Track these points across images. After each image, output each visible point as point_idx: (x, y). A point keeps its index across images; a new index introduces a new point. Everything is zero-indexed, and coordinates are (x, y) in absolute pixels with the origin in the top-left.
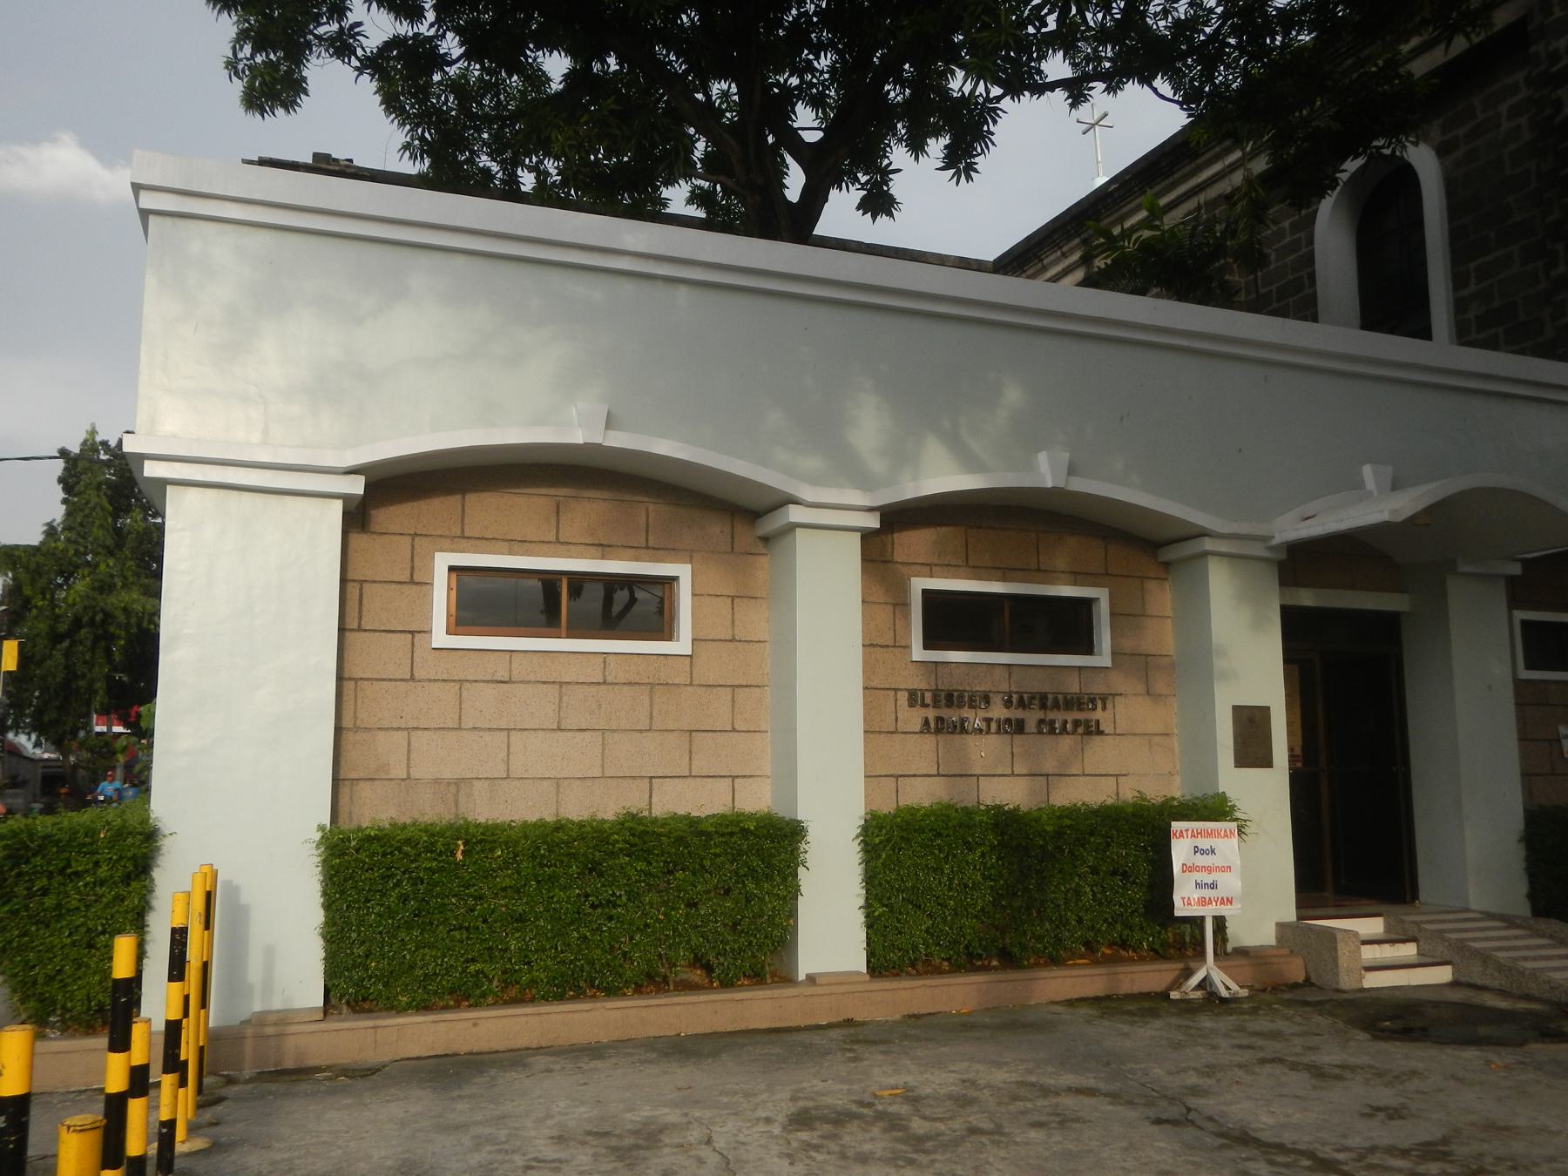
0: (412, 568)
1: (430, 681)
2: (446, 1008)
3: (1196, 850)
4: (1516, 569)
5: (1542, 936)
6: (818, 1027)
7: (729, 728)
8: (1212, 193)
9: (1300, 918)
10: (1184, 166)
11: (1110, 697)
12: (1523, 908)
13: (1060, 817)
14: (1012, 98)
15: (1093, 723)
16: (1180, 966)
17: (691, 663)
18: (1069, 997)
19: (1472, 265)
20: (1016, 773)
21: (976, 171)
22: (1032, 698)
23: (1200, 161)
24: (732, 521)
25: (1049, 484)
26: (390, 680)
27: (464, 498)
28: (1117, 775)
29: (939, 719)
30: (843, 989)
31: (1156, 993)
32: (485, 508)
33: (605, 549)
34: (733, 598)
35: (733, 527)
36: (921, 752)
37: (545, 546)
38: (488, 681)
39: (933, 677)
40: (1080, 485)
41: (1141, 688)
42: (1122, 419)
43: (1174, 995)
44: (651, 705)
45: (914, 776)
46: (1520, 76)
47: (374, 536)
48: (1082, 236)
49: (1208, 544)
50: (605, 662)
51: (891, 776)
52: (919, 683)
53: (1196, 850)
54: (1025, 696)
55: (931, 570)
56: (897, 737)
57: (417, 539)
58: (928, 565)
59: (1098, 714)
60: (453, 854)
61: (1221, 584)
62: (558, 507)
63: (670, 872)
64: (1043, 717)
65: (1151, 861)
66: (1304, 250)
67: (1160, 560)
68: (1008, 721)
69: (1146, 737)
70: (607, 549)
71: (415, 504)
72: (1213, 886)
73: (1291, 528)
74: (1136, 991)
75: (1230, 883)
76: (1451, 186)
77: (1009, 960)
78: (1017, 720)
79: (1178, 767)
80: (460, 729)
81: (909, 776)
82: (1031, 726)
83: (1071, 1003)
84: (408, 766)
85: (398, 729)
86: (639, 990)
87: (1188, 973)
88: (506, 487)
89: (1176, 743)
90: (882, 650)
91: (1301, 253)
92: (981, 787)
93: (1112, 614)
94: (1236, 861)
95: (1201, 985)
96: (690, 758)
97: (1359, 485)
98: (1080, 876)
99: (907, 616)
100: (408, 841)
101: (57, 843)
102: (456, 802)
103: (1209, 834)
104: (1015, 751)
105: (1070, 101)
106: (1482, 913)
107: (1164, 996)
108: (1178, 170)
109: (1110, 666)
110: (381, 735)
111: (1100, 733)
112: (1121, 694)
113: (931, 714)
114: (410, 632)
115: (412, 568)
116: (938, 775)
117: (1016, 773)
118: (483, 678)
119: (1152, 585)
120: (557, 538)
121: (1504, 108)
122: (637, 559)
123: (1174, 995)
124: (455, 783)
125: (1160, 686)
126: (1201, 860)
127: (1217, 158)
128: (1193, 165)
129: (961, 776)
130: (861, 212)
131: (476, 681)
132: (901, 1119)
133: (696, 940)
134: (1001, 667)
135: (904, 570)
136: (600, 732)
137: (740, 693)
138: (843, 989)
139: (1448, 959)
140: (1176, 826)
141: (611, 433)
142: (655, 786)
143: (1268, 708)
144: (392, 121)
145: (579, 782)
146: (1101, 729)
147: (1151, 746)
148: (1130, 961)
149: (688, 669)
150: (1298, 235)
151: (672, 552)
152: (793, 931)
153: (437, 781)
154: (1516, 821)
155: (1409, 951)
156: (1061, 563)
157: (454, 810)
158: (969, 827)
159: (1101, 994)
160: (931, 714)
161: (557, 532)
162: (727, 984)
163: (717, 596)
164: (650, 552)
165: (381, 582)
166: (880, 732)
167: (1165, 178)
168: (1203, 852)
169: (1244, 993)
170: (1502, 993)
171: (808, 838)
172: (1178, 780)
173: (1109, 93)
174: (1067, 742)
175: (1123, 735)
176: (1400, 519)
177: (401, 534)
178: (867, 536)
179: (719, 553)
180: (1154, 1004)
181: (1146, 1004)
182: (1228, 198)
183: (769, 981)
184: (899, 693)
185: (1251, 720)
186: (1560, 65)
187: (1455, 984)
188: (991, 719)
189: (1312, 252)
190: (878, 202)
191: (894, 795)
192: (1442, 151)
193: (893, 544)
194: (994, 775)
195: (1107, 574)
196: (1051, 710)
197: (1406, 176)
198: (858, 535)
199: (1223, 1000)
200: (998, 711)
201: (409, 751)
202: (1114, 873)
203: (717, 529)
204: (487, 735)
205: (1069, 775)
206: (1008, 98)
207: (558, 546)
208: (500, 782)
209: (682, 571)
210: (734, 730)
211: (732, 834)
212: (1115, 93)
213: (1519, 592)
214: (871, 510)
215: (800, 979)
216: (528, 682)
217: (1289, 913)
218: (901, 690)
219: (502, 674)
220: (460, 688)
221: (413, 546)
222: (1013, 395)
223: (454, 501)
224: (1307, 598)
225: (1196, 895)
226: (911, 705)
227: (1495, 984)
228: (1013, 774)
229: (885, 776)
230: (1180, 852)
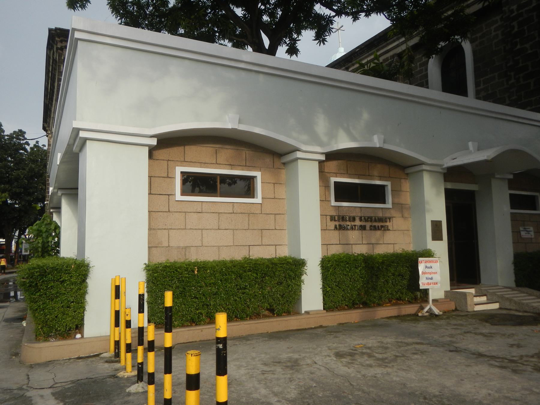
0: (168, 172)
1: (175, 212)
2: (188, 326)
3: (426, 267)
4: (511, 177)
5: (524, 293)
6: (311, 328)
7: (274, 228)
8: (391, 53)
9: (451, 289)
12: (513, 285)
13: (384, 257)
14: (338, 17)
16: (419, 305)
17: (261, 206)
18: (387, 316)
19: (482, 79)
21: (326, 41)
22: (368, 217)
23: (388, 42)
24: (273, 157)
25: (378, 146)
26: (161, 212)
27: (184, 147)
28: (394, 244)
29: (340, 225)
30: (319, 315)
31: (412, 314)
32: (193, 151)
33: (232, 166)
34: (274, 184)
35: (273, 160)
36: (335, 236)
37: (212, 165)
38: (194, 212)
40: (387, 147)
41: (400, 215)
42: (398, 125)
43: (420, 314)
44: (249, 220)
45: (332, 244)
46: (498, 18)
47: (154, 161)
48: (346, 66)
49: (424, 167)
50: (233, 206)
51: (325, 244)
52: (333, 213)
53: (426, 267)
54: (366, 217)
55: (336, 175)
56: (327, 231)
57: (169, 162)
58: (335, 173)
59: (388, 224)
60: (193, 271)
61: (427, 181)
62: (216, 151)
63: (264, 277)
64: (371, 224)
65: (410, 272)
66: (424, 73)
67: (405, 172)
68: (361, 226)
69: (402, 231)
70: (232, 166)
71: (168, 149)
72: (431, 279)
73: (449, 162)
74: (406, 314)
75: (437, 278)
76: (474, 53)
77: (365, 305)
78: (364, 226)
79: (412, 240)
80: (185, 229)
81: (331, 244)
82: (368, 227)
83: (388, 318)
84: (169, 242)
85: (165, 229)
86: (251, 318)
87: (422, 308)
88: (203, 144)
89: (411, 233)
91: (423, 74)
93: (392, 190)
94: (438, 270)
95: (427, 312)
96: (262, 239)
97: (467, 148)
98: (388, 277)
99: (329, 191)
100: (179, 268)
101: (57, 270)
102: (185, 254)
103: (430, 262)
105: (353, 19)
106: (503, 286)
107: (416, 315)
108: (381, 45)
109: (391, 207)
110: (159, 232)
112: (394, 217)
113: (337, 223)
114: (167, 195)
115: (168, 172)
116: (340, 244)
118: (193, 211)
119: (403, 181)
120: (216, 162)
121: (493, 28)
122: (243, 170)
123: (420, 314)
124: (185, 248)
125: (406, 215)
126: (428, 270)
127: (394, 41)
128: (386, 43)
130: (287, 54)
131: (190, 212)
132: (371, 354)
133: (271, 300)
135: (328, 175)
136: (232, 230)
137: (277, 216)
138: (319, 315)
139: (498, 301)
140: (420, 259)
141: (240, 125)
142: (251, 249)
143: (441, 221)
144: (113, 16)
145: (225, 247)
147: (403, 234)
148: (401, 304)
149: (260, 208)
150: (422, 68)
151: (254, 168)
152: (300, 296)
153: (178, 247)
154: (511, 258)
155: (484, 299)
156: (376, 173)
157: (184, 257)
158: (357, 261)
159: (396, 315)
160: (337, 223)
161: (216, 160)
162: (279, 315)
163: (269, 183)
164: (247, 167)
165: (157, 177)
167: (376, 47)
168: (428, 268)
169: (441, 313)
170: (516, 310)
171: (307, 265)
172: (412, 245)
173: (366, 17)
174: (378, 233)
176: (490, 158)
177: (163, 160)
178: (321, 162)
179: (269, 168)
180: (415, 317)
181: (413, 318)
182: (400, 55)
183: (292, 314)
184: (327, 216)
185: (436, 225)
186: (514, 14)
187: (500, 308)
188: (356, 225)
189: (427, 73)
190: (293, 50)
192: (472, 42)
193: (324, 166)
194: (357, 244)
195: (390, 177)
196: (374, 222)
197: (460, 50)
198: (318, 162)
199: (436, 316)
200: (358, 223)
201: (169, 237)
202: (399, 275)
203: (268, 160)
204: (195, 231)
205: (380, 244)
206: (337, 16)
207: (217, 165)
208: (200, 247)
209: (258, 174)
210: (275, 229)
211: (283, 264)
212: (368, 17)
213: (512, 184)
214: (322, 153)
215: (303, 313)
216: (208, 213)
217: (448, 288)
218: (328, 215)
219: (199, 210)
220: (185, 215)
221: (168, 164)
222: (366, 116)
223: (181, 148)
224: (450, 186)
225: (427, 281)
226: (331, 220)
227: (514, 308)
228: (362, 244)
230: (421, 268)
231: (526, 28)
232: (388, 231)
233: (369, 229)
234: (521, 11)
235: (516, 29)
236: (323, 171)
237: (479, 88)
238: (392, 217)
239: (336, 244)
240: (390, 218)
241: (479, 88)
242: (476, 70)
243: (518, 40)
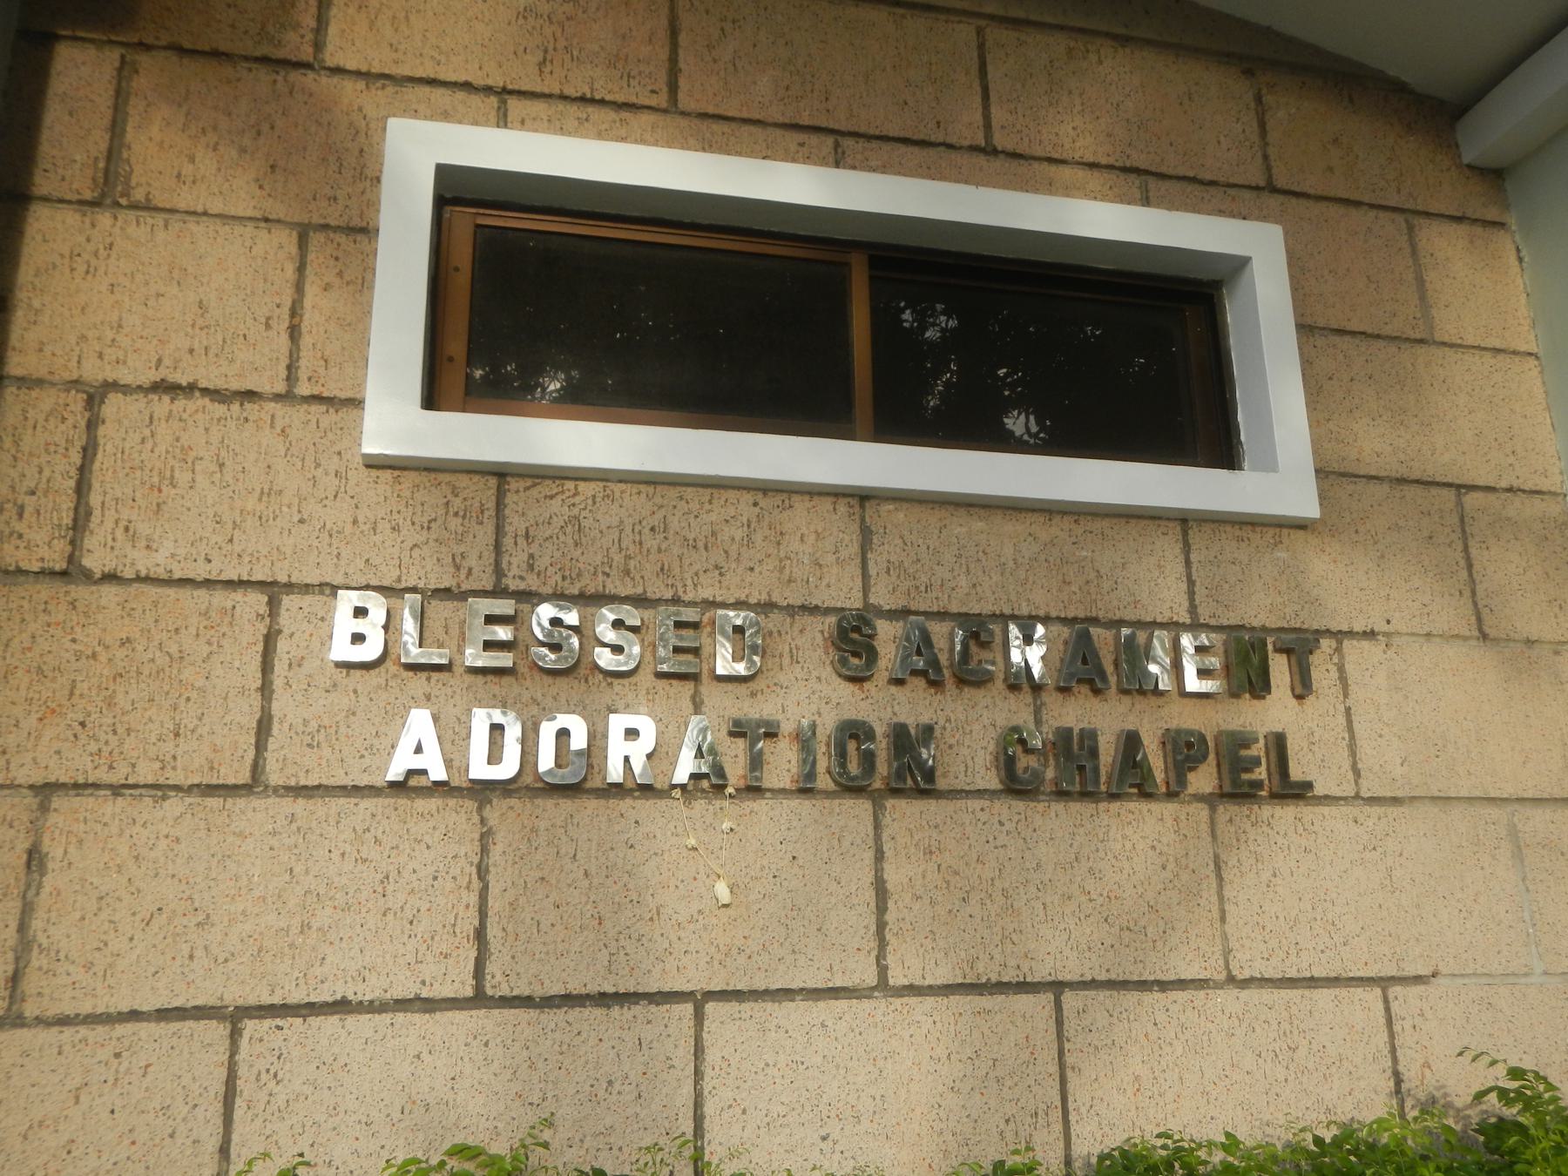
11: (1326, 644)
15: (1258, 749)
20: (897, 978)
28: (1384, 983)
39: (486, 534)
41: (1451, 614)
45: (341, 1006)
54: (938, 630)
58: (488, 90)
67: (1467, 158)
90: (219, 409)
92: (712, 1056)
93: (1305, 329)
104: (892, 876)
109: (1309, 508)
111: (1294, 792)
112: (1370, 635)
116: (480, 999)
117: (897, 978)
129: (604, 999)
134: (826, 504)
146: (1296, 773)
147: (1518, 854)
166: (161, 790)
175: (1396, 801)
191: (213, 1110)
194: (787, 994)
205: (1164, 986)
228: (883, 986)
229: (163, 1015)
232: (1285, 814)
233: (992, 781)
236: (306, 54)
238: (1340, 635)
239: (402, 1005)
240: (1299, 647)
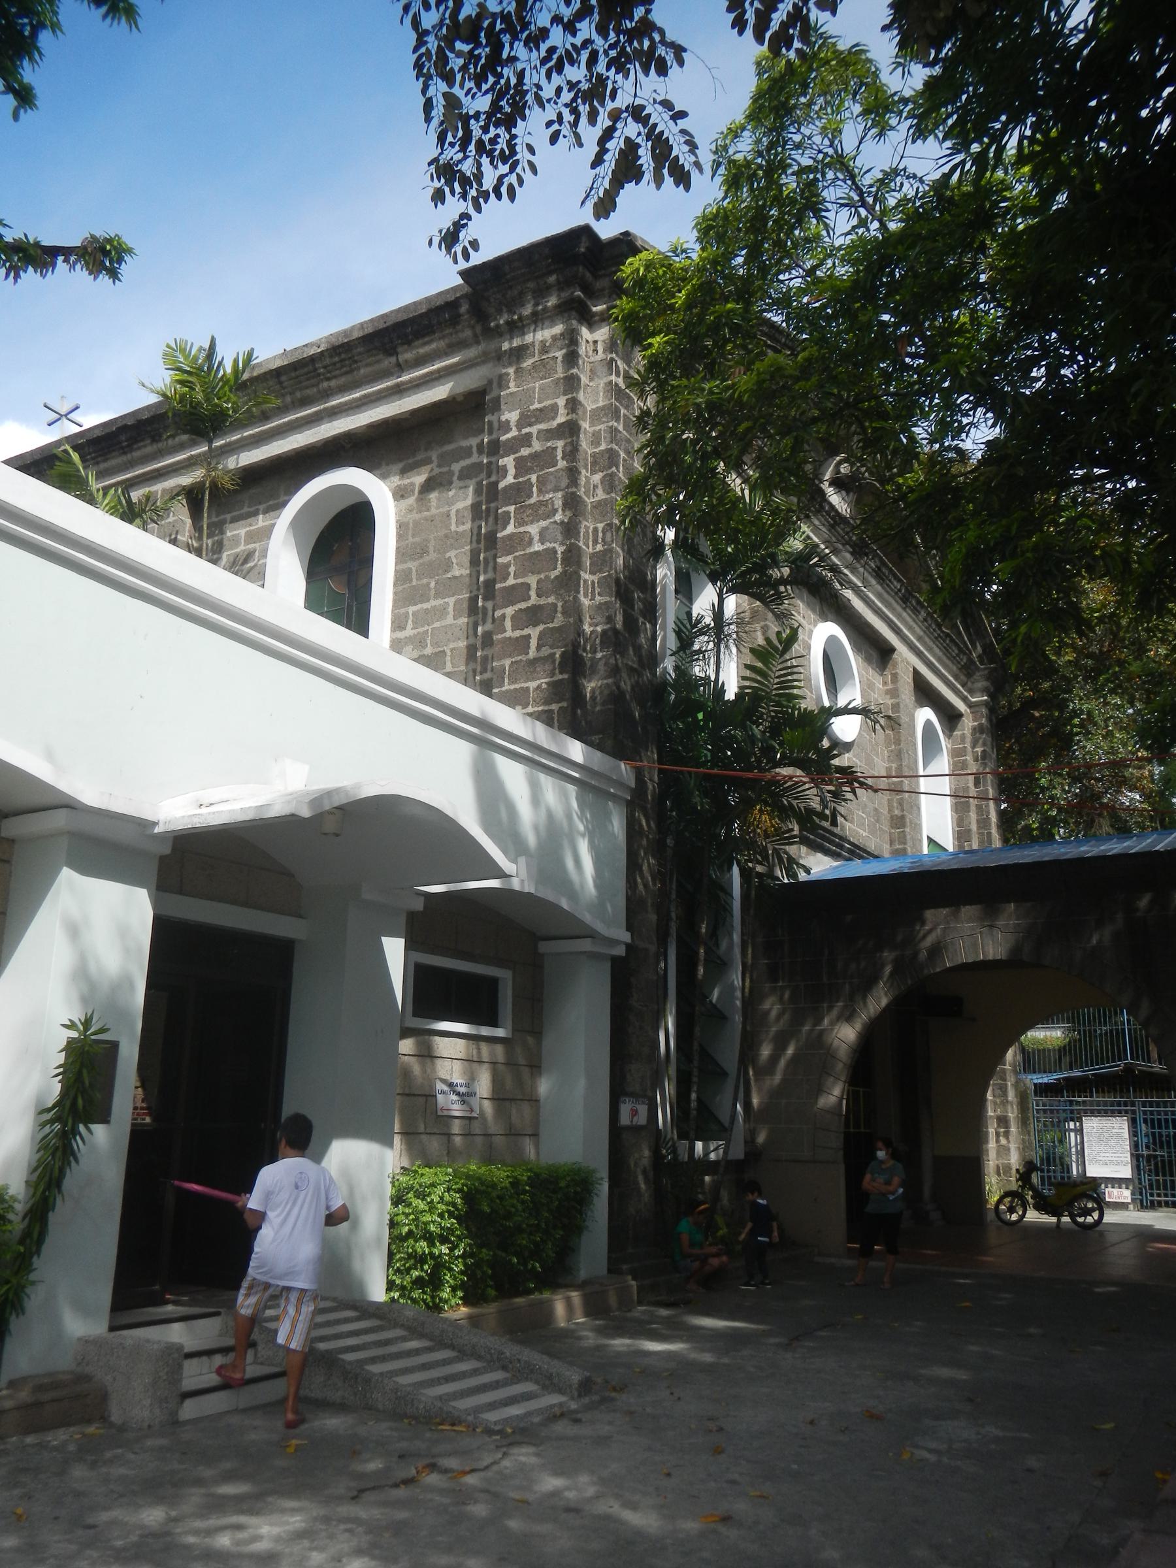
10: (145, 446)
46: (473, 442)
76: (402, 527)
108: (139, 448)
167: (125, 453)
186: (509, 436)
231: (534, 478)
234: (526, 430)
235: (510, 479)
237: (400, 635)
241: (400, 635)
242: (401, 577)
243: (512, 508)
